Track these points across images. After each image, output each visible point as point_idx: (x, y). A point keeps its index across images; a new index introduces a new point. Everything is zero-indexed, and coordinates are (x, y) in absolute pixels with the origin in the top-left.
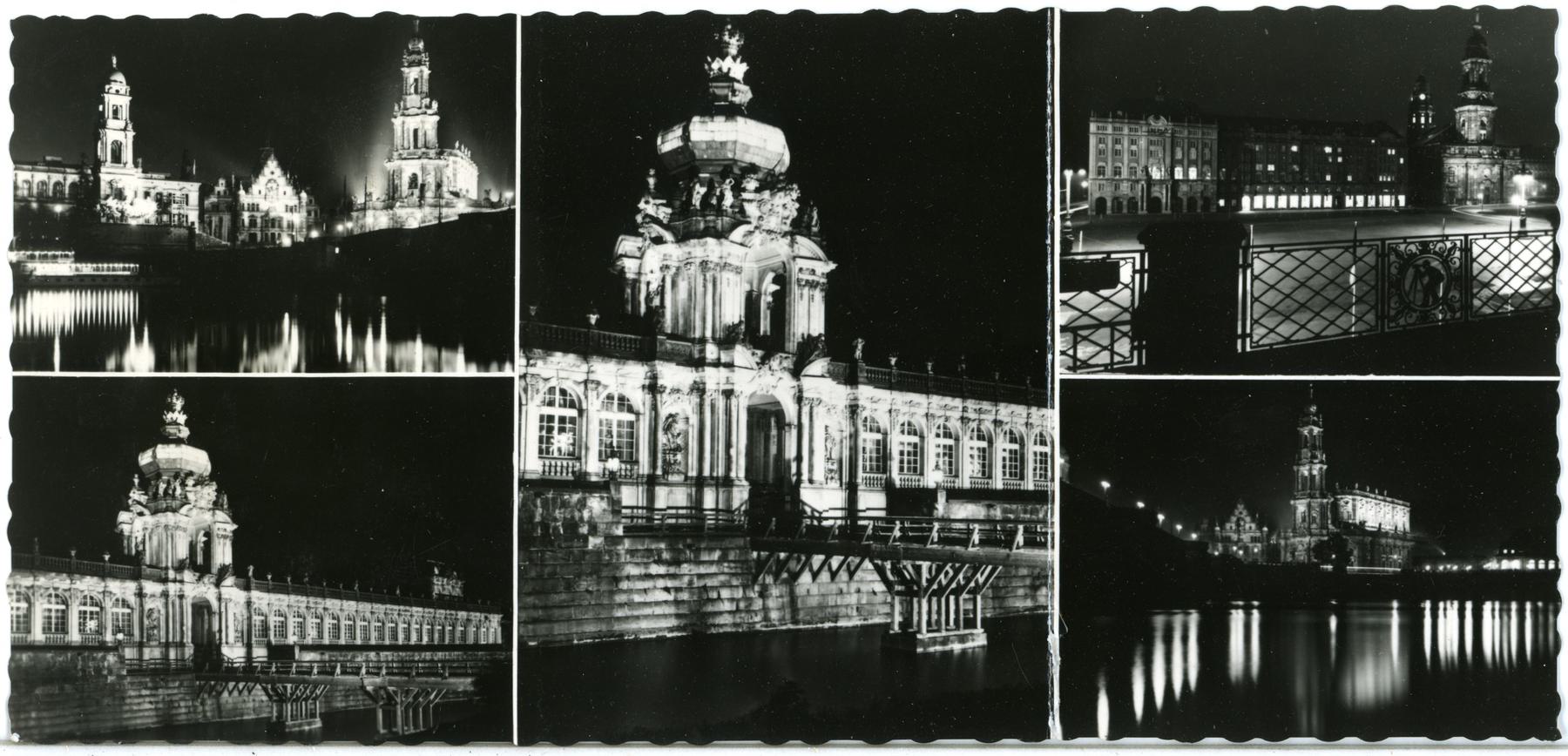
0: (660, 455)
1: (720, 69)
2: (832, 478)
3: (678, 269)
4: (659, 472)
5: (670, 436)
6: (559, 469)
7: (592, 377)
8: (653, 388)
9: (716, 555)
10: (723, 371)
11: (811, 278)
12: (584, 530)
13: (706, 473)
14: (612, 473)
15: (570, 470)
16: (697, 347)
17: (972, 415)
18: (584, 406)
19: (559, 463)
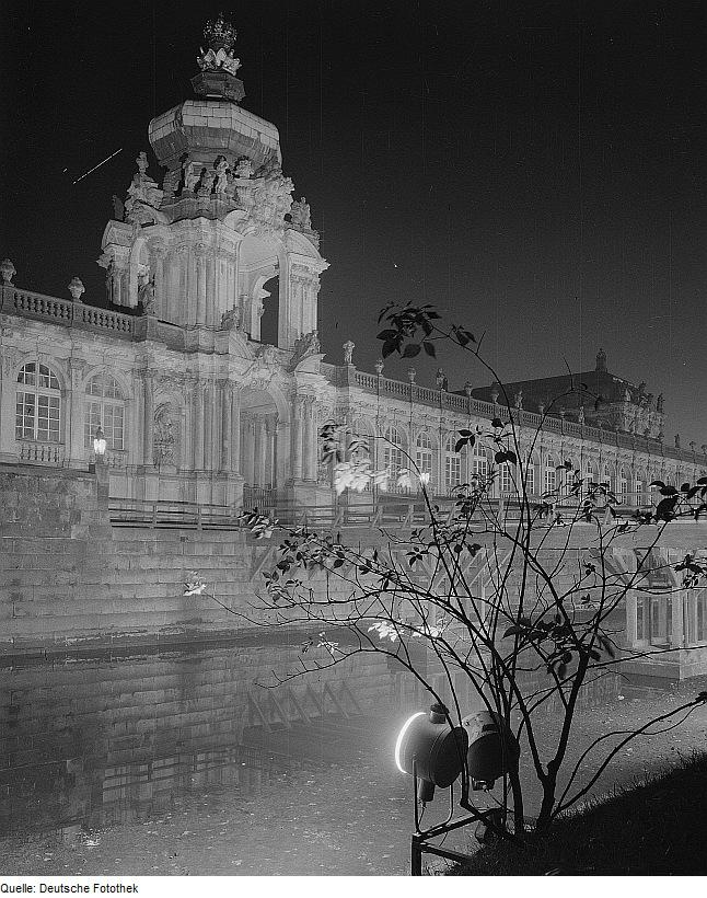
0: (151, 443)
1: (213, 63)
2: (323, 480)
3: (169, 254)
4: (150, 462)
5: (162, 426)
6: (39, 454)
7: (77, 355)
9: (210, 550)
10: (217, 361)
11: (304, 275)
12: (65, 517)
13: (200, 466)
14: (99, 457)
15: (52, 456)
17: (449, 427)
18: (68, 387)
19: (39, 448)
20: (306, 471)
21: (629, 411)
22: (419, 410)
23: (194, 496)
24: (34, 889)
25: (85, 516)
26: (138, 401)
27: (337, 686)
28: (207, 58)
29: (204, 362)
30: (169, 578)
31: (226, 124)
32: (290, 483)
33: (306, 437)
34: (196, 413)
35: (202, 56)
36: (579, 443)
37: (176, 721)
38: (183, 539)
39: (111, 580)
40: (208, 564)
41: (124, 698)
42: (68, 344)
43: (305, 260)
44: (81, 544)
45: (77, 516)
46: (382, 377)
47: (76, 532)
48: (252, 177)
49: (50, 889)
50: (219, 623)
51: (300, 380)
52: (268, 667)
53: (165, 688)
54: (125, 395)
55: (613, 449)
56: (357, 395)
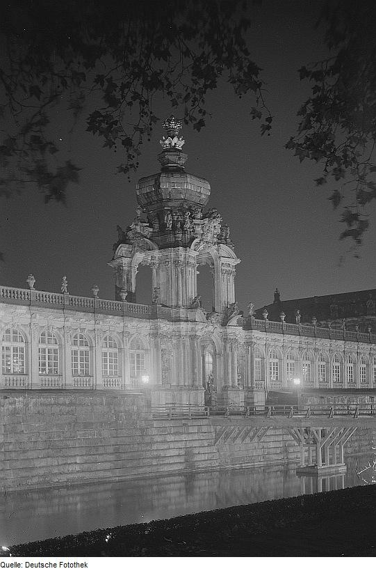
10: (190, 325)
17: (304, 346)
22: (288, 337)
24: (22, 566)
29: (183, 326)
42: (122, 324)
46: (267, 321)
49: (32, 565)
51: (229, 330)
56: (256, 334)
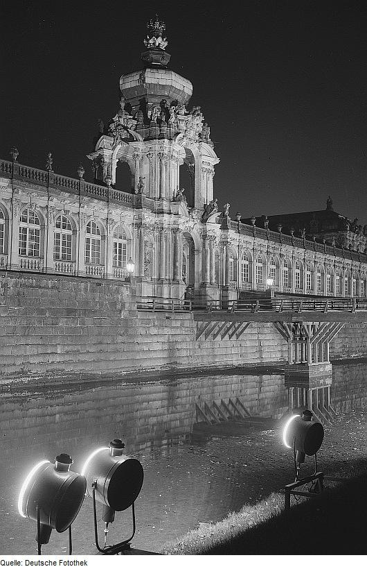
8: (139, 225)
9: (178, 324)
10: (173, 218)
12: (119, 307)
16: (157, 203)
20: (211, 279)
21: (350, 236)
22: (259, 241)
23: (161, 294)
24: (21, 564)
25: (127, 305)
26: (135, 241)
27: (234, 400)
28: (151, 41)
29: (166, 218)
30: (161, 339)
31: (169, 83)
32: (203, 285)
33: (211, 257)
34: (160, 246)
35: (148, 40)
36: (333, 258)
37: (165, 418)
38: (168, 318)
39: (139, 340)
40: (178, 332)
41: (145, 404)
43: (207, 158)
44: (126, 320)
45: (123, 305)
47: (124, 314)
48: (186, 114)
49: (32, 563)
50: (184, 364)
52: (205, 389)
53: (162, 400)
54: (128, 237)
55: (350, 262)
56: (232, 234)
